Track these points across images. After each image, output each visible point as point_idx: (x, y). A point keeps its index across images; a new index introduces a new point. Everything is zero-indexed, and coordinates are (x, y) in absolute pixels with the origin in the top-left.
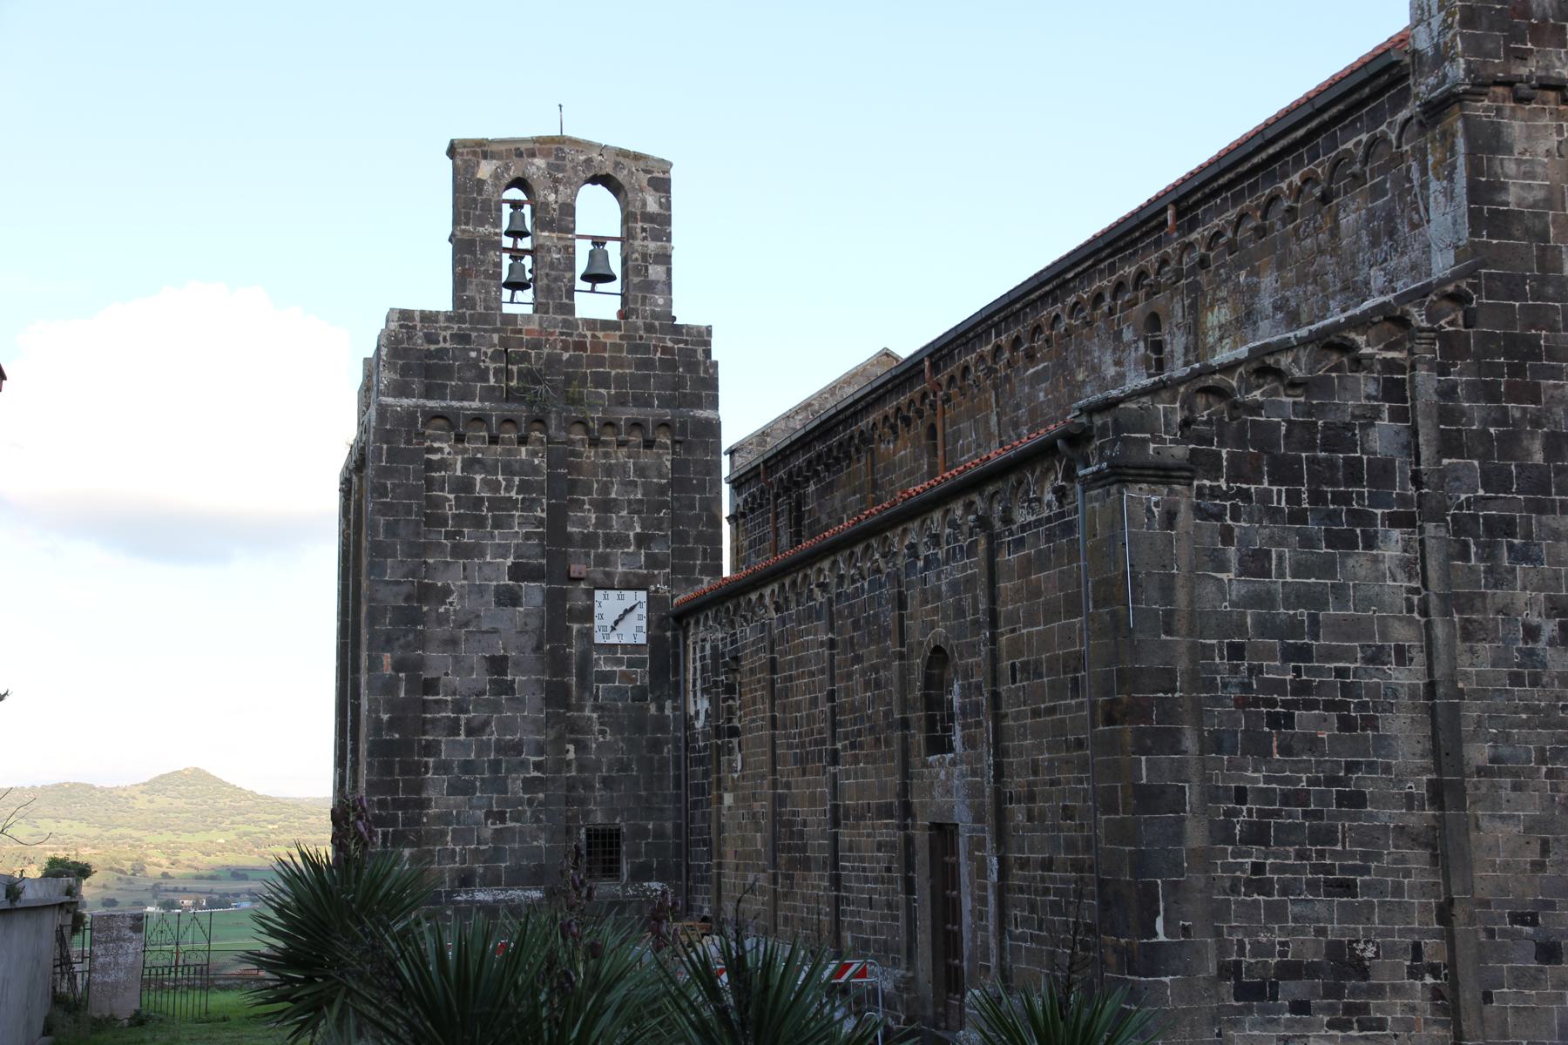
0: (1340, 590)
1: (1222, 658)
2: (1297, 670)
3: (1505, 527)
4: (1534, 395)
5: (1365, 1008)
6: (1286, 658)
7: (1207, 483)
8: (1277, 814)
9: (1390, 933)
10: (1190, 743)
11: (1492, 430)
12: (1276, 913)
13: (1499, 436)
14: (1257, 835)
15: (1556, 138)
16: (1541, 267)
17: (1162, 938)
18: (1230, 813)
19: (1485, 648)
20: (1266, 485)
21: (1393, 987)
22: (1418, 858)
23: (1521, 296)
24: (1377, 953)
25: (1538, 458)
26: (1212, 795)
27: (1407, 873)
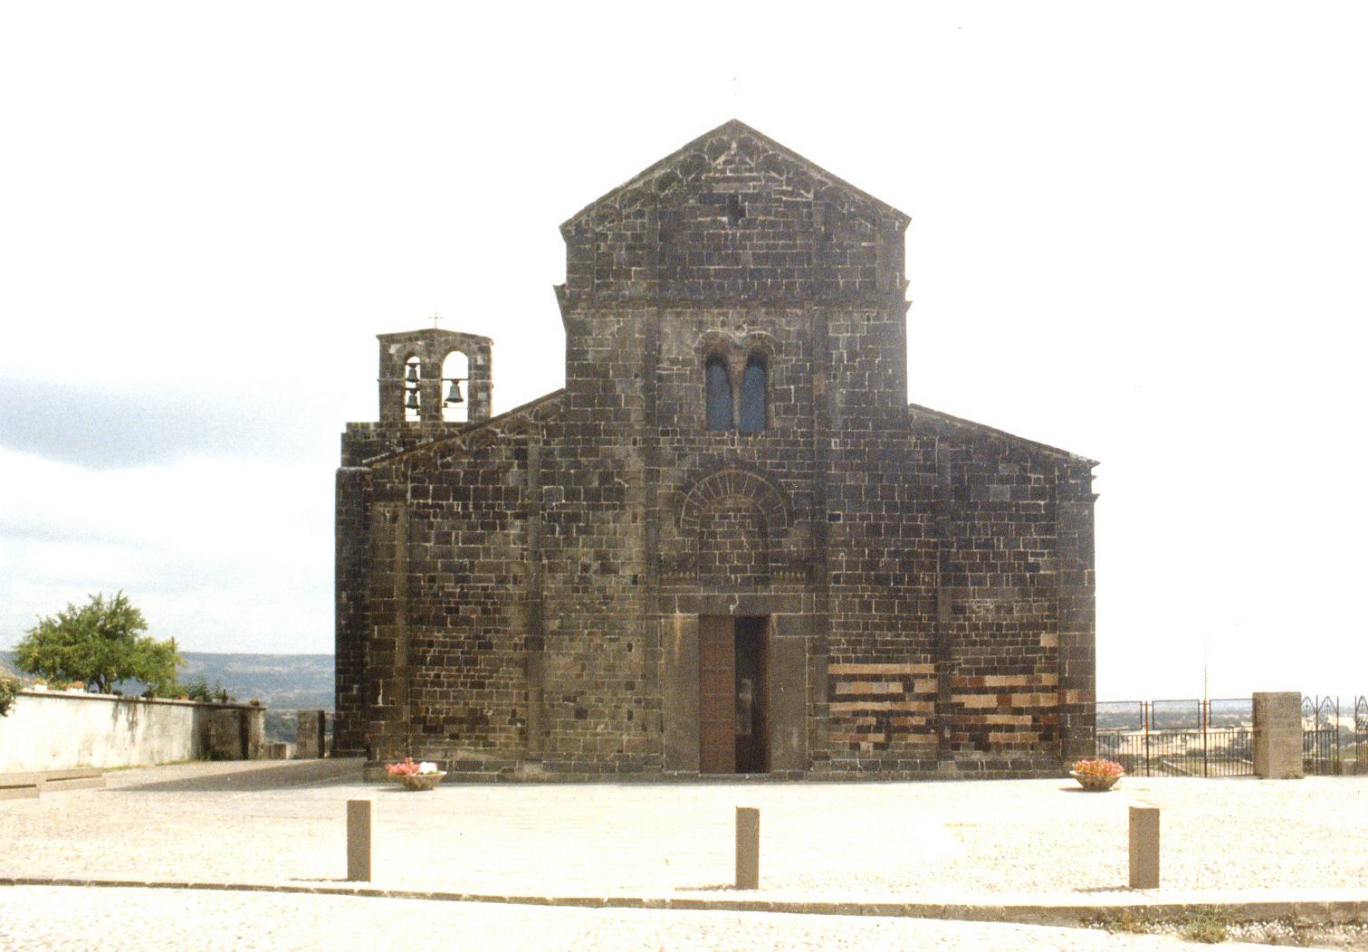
0: (487, 551)
1: (425, 582)
2: (462, 588)
3: (574, 518)
4: (595, 452)
5: (485, 738)
6: (457, 582)
7: (421, 501)
8: (448, 652)
9: (502, 705)
10: (400, 621)
11: (572, 471)
12: (445, 695)
13: (576, 475)
14: (438, 661)
15: (617, 326)
16: (604, 390)
17: (381, 704)
18: (424, 652)
19: (560, 576)
20: (451, 501)
21: (501, 729)
22: (517, 673)
23: (592, 405)
24: (493, 714)
25: (596, 484)
26: (413, 643)
27: (511, 679)
